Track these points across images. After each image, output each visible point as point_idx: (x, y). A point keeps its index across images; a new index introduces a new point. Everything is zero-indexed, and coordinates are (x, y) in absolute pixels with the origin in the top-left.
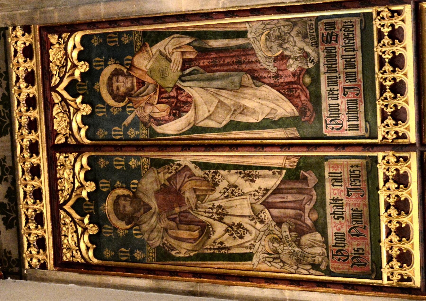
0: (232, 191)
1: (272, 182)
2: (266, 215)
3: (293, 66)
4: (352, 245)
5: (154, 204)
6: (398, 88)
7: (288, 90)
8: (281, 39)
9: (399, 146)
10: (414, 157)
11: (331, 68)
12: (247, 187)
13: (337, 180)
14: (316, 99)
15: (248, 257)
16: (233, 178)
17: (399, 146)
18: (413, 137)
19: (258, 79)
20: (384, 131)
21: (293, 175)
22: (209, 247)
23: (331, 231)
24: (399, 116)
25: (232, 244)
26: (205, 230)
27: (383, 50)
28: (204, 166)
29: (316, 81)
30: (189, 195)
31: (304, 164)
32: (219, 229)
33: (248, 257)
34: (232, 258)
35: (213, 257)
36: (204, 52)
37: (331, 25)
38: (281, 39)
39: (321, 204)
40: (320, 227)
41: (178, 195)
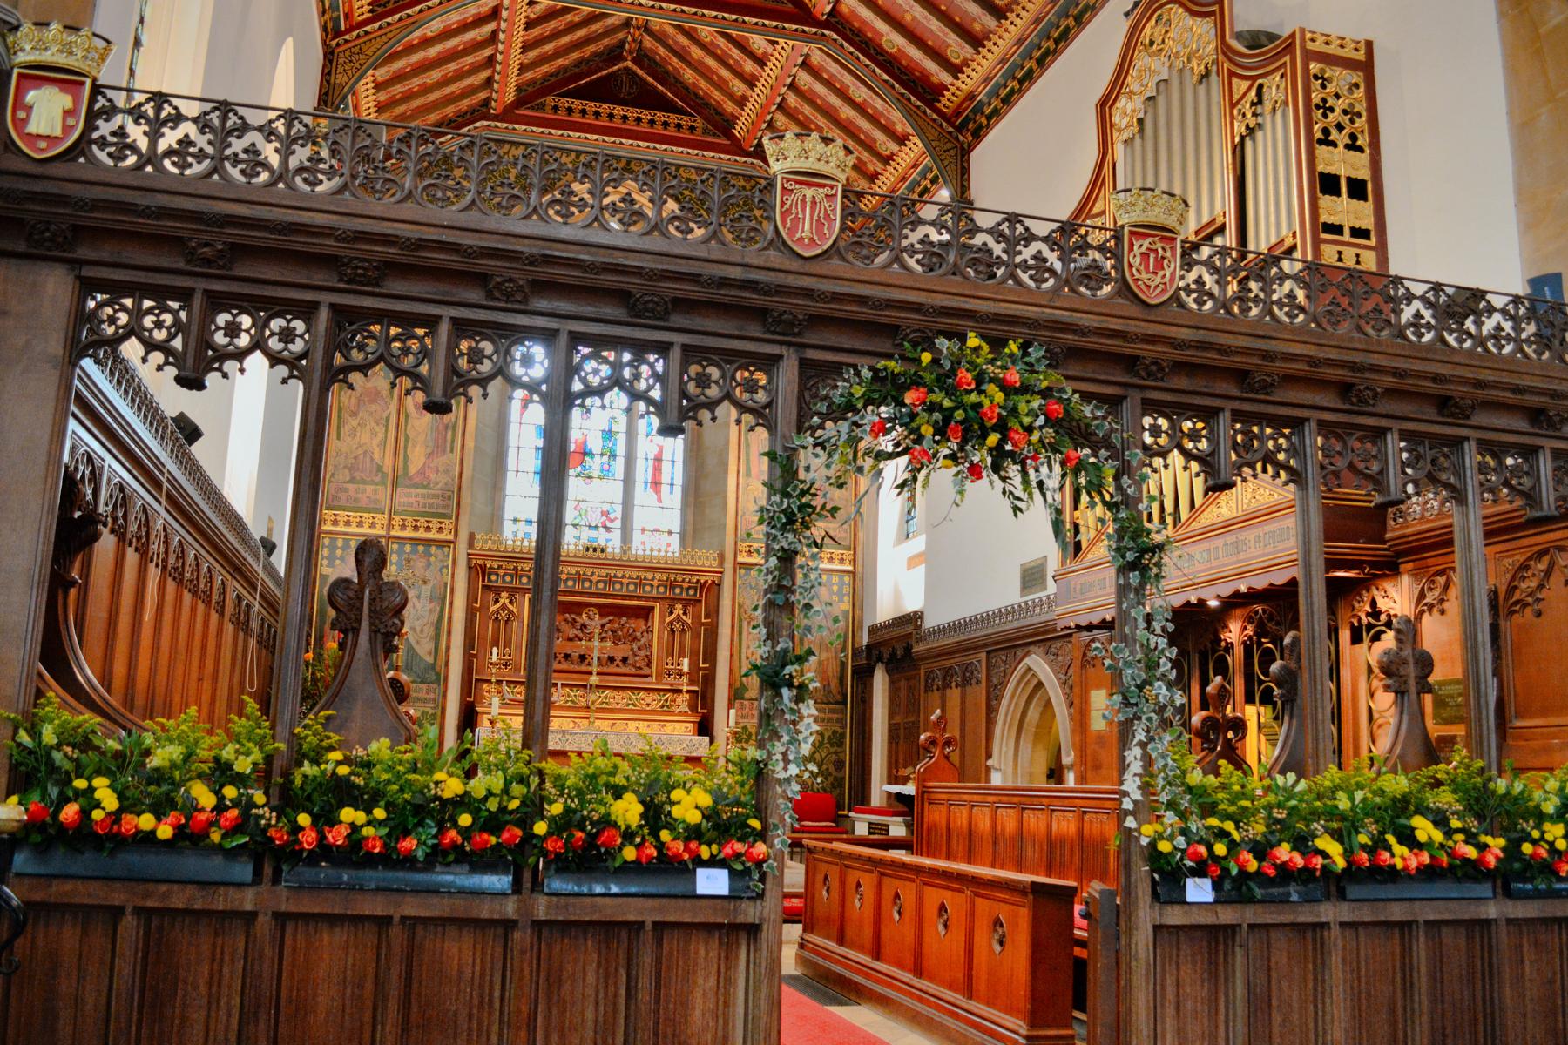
0: (374, 433)
1: (376, 456)
2: (360, 451)
3: (433, 476)
4: (343, 496)
5: (369, 385)
6: (416, 528)
7: (421, 472)
8: (447, 471)
9: (390, 526)
10: (383, 533)
11: (429, 496)
12: (375, 442)
13: (375, 492)
14: (416, 486)
15: (339, 438)
16: (381, 436)
17: (390, 526)
18: (393, 533)
19: (429, 455)
20: (397, 520)
21: (379, 468)
22: (346, 415)
23: (350, 486)
24: (403, 527)
25: (345, 430)
26: (354, 414)
27: (434, 524)
28: (388, 420)
29: (425, 487)
30: (373, 407)
31: (385, 475)
32: (353, 422)
33: (339, 438)
34: (339, 428)
35: (339, 417)
36: (446, 427)
37: (450, 498)
38: (447, 471)
39: (364, 482)
40: (352, 480)
41: (372, 401)
